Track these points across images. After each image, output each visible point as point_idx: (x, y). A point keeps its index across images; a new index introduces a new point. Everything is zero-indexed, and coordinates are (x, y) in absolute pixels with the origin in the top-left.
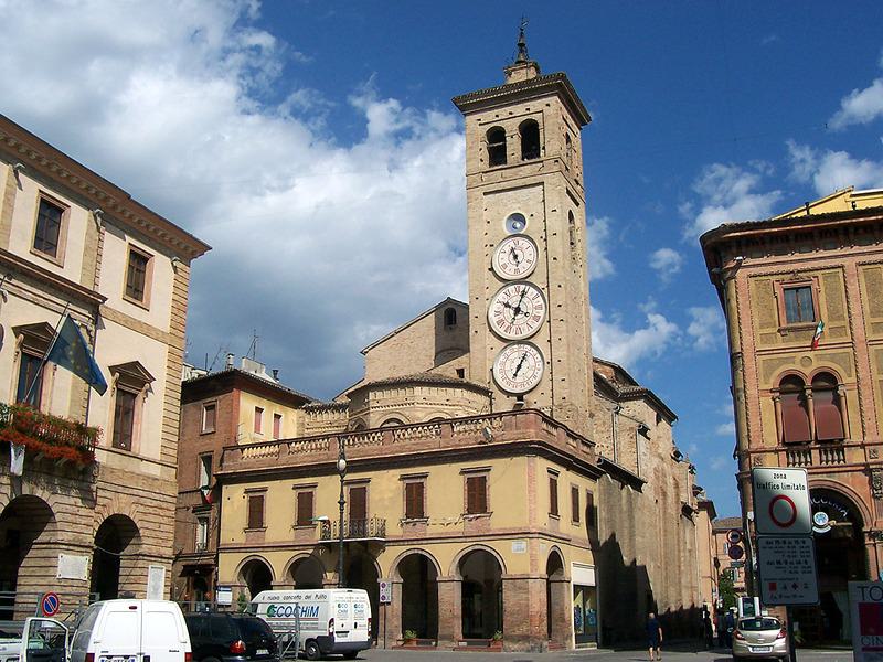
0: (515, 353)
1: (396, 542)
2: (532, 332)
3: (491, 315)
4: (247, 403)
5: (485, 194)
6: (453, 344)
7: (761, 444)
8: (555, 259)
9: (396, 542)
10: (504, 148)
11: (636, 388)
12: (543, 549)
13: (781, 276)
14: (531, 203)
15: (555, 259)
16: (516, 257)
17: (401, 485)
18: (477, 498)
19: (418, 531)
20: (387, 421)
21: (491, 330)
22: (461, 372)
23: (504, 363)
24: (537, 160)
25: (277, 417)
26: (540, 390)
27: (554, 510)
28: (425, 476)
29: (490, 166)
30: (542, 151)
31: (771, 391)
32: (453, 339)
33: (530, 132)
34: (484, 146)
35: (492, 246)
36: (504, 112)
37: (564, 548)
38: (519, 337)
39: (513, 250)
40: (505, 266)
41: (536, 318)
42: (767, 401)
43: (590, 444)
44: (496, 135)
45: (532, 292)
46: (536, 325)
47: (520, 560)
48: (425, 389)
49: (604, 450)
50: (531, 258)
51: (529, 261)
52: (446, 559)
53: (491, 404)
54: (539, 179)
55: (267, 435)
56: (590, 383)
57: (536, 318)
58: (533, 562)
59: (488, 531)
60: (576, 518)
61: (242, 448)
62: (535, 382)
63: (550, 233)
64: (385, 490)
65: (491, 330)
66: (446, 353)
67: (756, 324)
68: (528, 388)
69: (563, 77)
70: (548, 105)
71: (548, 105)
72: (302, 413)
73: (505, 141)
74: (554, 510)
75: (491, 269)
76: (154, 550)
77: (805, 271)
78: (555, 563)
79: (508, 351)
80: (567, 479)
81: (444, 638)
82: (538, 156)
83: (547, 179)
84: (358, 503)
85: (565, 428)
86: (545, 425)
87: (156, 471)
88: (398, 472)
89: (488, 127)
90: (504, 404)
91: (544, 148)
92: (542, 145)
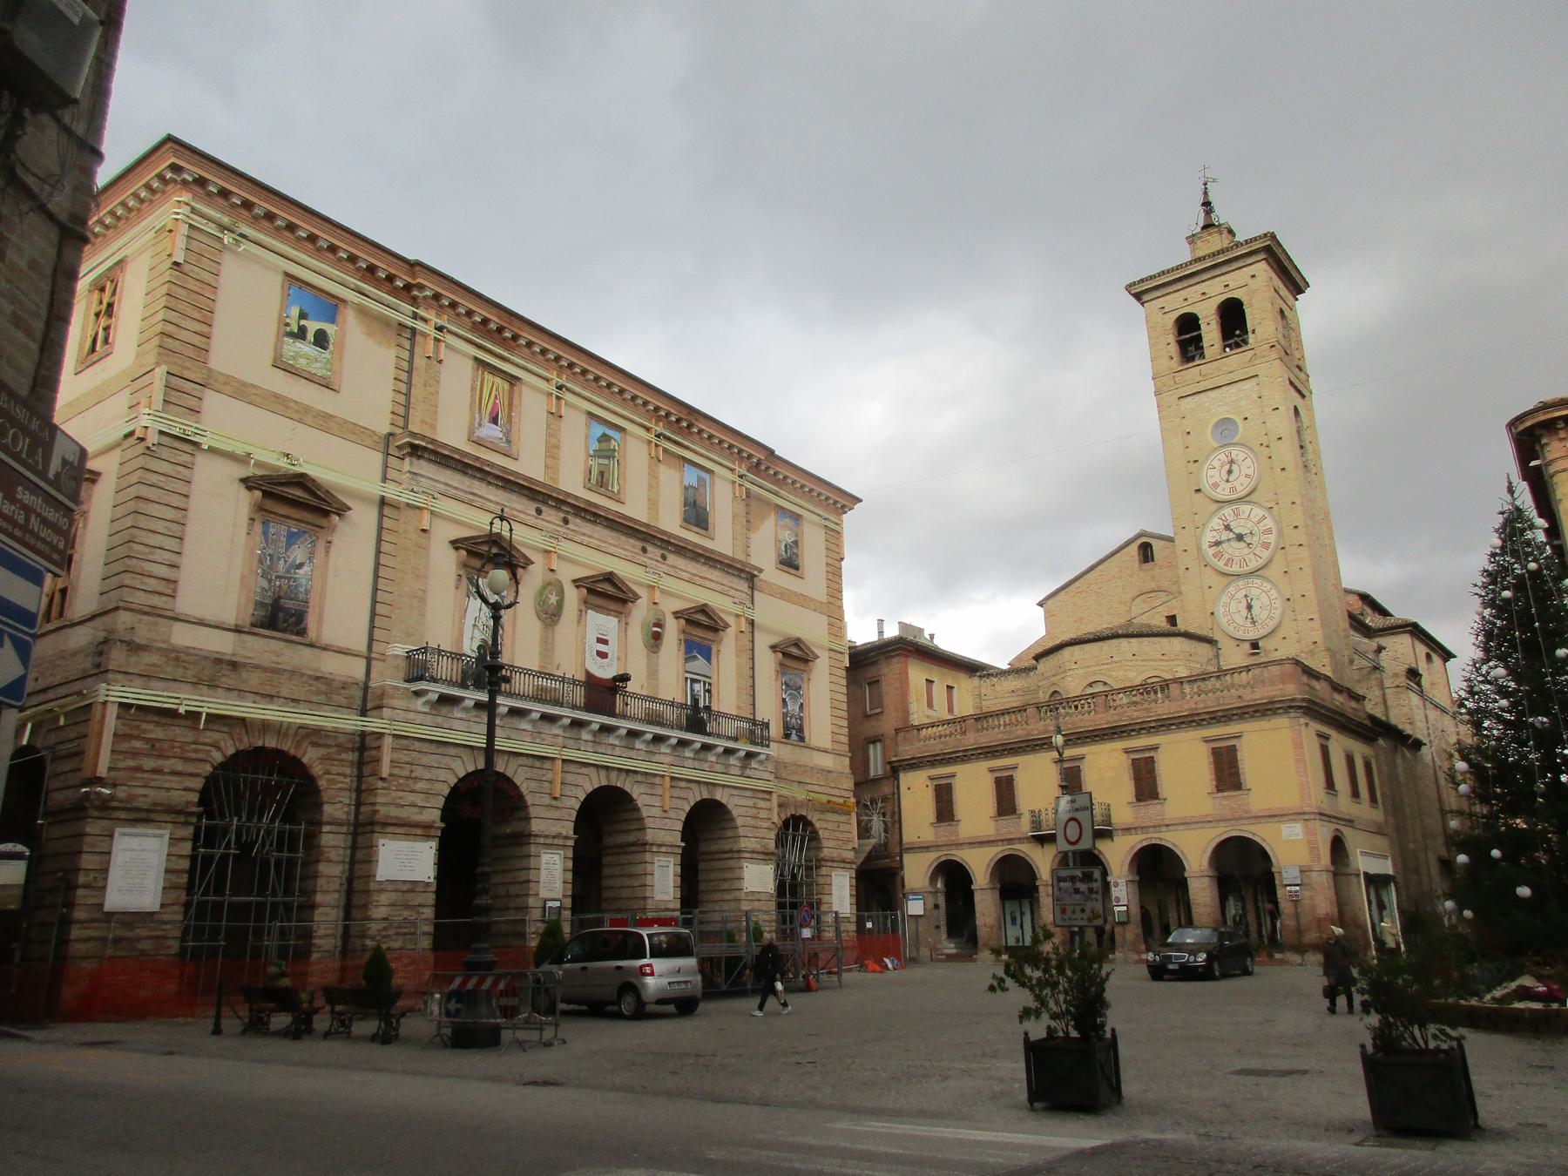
0: (1238, 590)
1: (1127, 830)
2: (1261, 562)
3: (1205, 546)
4: (917, 674)
6: (1153, 585)
9: (1127, 830)
10: (1199, 338)
11: (1389, 621)
12: (1324, 833)
16: (1230, 472)
17: (1124, 762)
18: (1227, 771)
19: (1151, 810)
20: (1090, 685)
22: (1172, 620)
23: (1227, 605)
25: (950, 688)
26: (1280, 635)
27: (1330, 784)
28: (1155, 748)
32: (1153, 578)
33: (1233, 317)
36: (1193, 293)
37: (1347, 832)
38: (1246, 569)
40: (1215, 485)
41: (1266, 546)
43: (1359, 698)
44: (1188, 325)
45: (1258, 512)
46: (1265, 554)
47: (1294, 850)
49: (1373, 708)
50: (1250, 472)
51: (1247, 476)
52: (1195, 852)
53: (1217, 656)
55: (941, 712)
56: (1344, 623)
57: (1266, 546)
58: (1313, 849)
60: (1355, 794)
61: (919, 728)
62: (1272, 625)
64: (1105, 771)
68: (1263, 632)
69: (1273, 237)
73: (1199, 328)
74: (1330, 784)
76: (835, 854)
78: (1338, 847)
79: (1231, 589)
80: (1340, 744)
83: (1261, 369)
84: (1071, 781)
85: (1327, 679)
86: (1305, 679)
87: (826, 761)
88: (1119, 745)
90: (1234, 656)
92: (1250, 328)
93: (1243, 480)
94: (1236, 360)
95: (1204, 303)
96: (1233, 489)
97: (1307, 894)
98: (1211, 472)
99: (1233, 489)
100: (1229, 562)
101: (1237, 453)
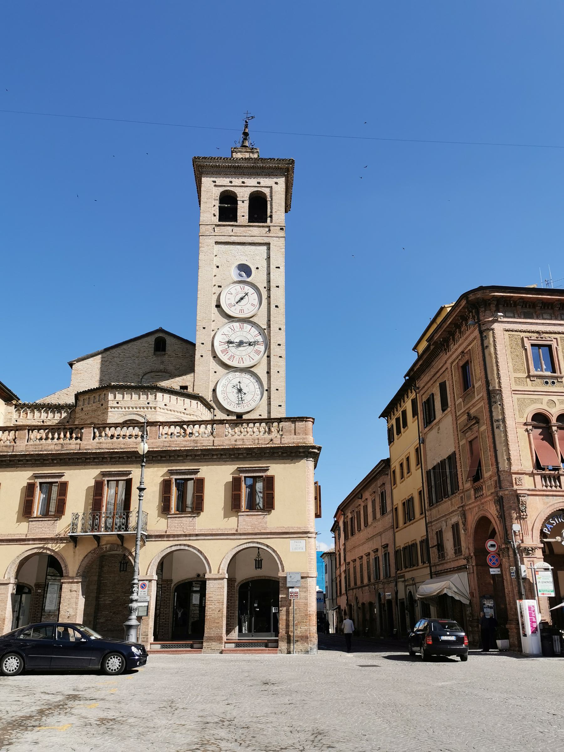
5: (217, 243)
6: (162, 367)
7: (520, 467)
8: (277, 306)
13: (530, 334)
14: (258, 257)
15: (277, 306)
21: (215, 357)
24: (265, 224)
29: (219, 221)
30: (269, 219)
31: (525, 424)
32: (162, 362)
34: (217, 204)
35: (220, 287)
38: (241, 365)
39: (247, 294)
42: (522, 430)
48: (167, 396)
54: (266, 240)
59: (265, 529)
63: (273, 284)
65: (215, 357)
66: (153, 374)
67: (511, 369)
70: (276, 183)
71: (276, 183)
72: (12, 409)
73: (237, 204)
75: (218, 306)
77: (547, 333)
81: (211, 639)
82: (266, 222)
89: (222, 189)
91: (271, 216)
92: (269, 214)
93: (249, 306)
94: (256, 232)
95: (244, 188)
96: (241, 311)
97: (303, 594)
98: (229, 296)
99: (241, 311)
100: (232, 357)
101: (248, 289)
